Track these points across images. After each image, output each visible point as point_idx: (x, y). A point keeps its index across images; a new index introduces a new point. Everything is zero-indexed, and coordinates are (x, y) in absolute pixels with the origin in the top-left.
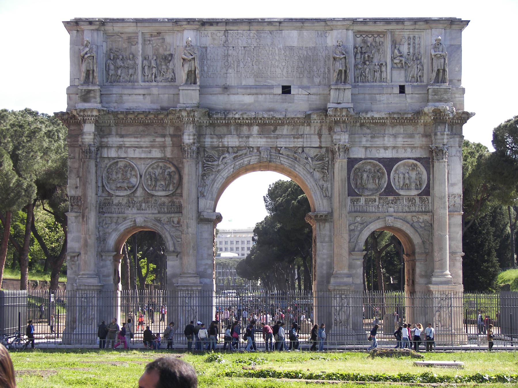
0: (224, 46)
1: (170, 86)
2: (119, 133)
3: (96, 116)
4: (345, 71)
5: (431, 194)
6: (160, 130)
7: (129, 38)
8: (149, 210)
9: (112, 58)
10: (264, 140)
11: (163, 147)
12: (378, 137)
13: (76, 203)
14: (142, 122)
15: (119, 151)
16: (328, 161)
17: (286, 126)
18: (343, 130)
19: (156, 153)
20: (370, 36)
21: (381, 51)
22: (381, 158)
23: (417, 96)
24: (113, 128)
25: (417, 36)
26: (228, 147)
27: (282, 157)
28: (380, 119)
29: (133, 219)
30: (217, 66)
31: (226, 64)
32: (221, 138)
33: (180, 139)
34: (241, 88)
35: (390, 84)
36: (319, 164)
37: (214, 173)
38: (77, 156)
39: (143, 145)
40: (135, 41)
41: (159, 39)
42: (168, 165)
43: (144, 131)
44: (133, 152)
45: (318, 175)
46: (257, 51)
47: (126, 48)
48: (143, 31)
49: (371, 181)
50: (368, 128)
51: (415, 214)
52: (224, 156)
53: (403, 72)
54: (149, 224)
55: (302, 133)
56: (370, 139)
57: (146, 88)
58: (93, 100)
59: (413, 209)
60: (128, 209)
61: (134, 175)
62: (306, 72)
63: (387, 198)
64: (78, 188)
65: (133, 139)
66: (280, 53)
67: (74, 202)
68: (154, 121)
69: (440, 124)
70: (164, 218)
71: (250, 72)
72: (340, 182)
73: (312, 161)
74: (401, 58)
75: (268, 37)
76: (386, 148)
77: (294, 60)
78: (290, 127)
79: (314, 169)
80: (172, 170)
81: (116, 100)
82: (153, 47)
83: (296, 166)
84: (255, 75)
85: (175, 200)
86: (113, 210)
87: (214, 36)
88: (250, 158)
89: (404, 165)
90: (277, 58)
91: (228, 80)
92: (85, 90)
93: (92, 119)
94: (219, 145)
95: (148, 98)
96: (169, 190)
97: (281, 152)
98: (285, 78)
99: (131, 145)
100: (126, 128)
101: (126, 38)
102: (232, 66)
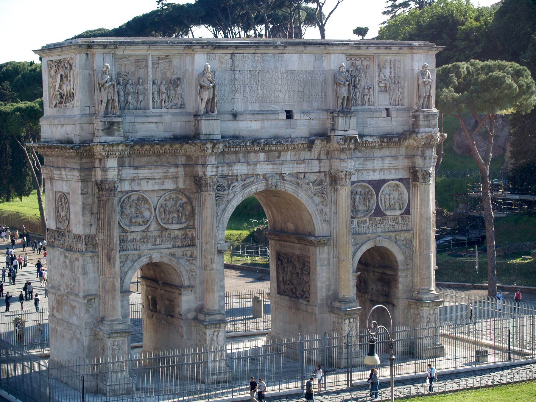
0: (231, 70)
1: (180, 112)
2: (132, 164)
3: (121, 150)
4: (348, 98)
5: (411, 213)
6: (172, 160)
7: (137, 61)
8: (164, 245)
9: (121, 83)
10: (271, 167)
11: (175, 178)
12: (369, 160)
13: (91, 242)
14: (156, 152)
15: (132, 183)
16: (327, 186)
17: (289, 152)
18: (349, 157)
19: (169, 185)
20: (358, 59)
21: (367, 74)
22: (370, 181)
23: (401, 119)
24: (125, 159)
25: (397, 60)
26: (237, 176)
27: (287, 183)
28: (372, 142)
29: (149, 255)
30: (225, 90)
31: (234, 88)
32: (231, 166)
33: (192, 168)
34: (249, 114)
35: (377, 107)
36: (318, 189)
37: (224, 202)
38: (90, 190)
39: (156, 176)
40: (143, 64)
41: (167, 62)
42: (180, 196)
43: (156, 162)
44: (146, 183)
45: (318, 200)
46: (262, 75)
47: (134, 72)
48: (152, 54)
49: (362, 203)
50: (360, 151)
51: (398, 233)
52: (233, 185)
53: (387, 95)
54: (165, 259)
55: (303, 158)
56: (361, 162)
57: (159, 116)
58: (117, 133)
59: (397, 228)
60: (143, 245)
61: (147, 209)
62: (306, 96)
63: (375, 219)
64: (93, 225)
65: (146, 171)
66: (283, 77)
67: (89, 241)
68: (168, 151)
69: (428, 148)
70: (179, 252)
71: (255, 97)
72: (347, 209)
73: (313, 186)
74: (386, 82)
75: (272, 60)
76: (374, 171)
77: (295, 85)
78: (293, 153)
79: (315, 195)
80: (183, 202)
81: (129, 130)
82: (161, 70)
83: (299, 192)
84: (260, 100)
85: (188, 233)
86: (129, 247)
87: (222, 60)
88: (257, 186)
89: (389, 186)
90: (280, 82)
91: (235, 105)
92: (108, 122)
93: (117, 154)
94: (229, 173)
95: (161, 126)
96: (181, 223)
97: (285, 178)
98: (287, 103)
99: (144, 177)
100: (139, 159)
101: (134, 61)
102: (239, 90)
